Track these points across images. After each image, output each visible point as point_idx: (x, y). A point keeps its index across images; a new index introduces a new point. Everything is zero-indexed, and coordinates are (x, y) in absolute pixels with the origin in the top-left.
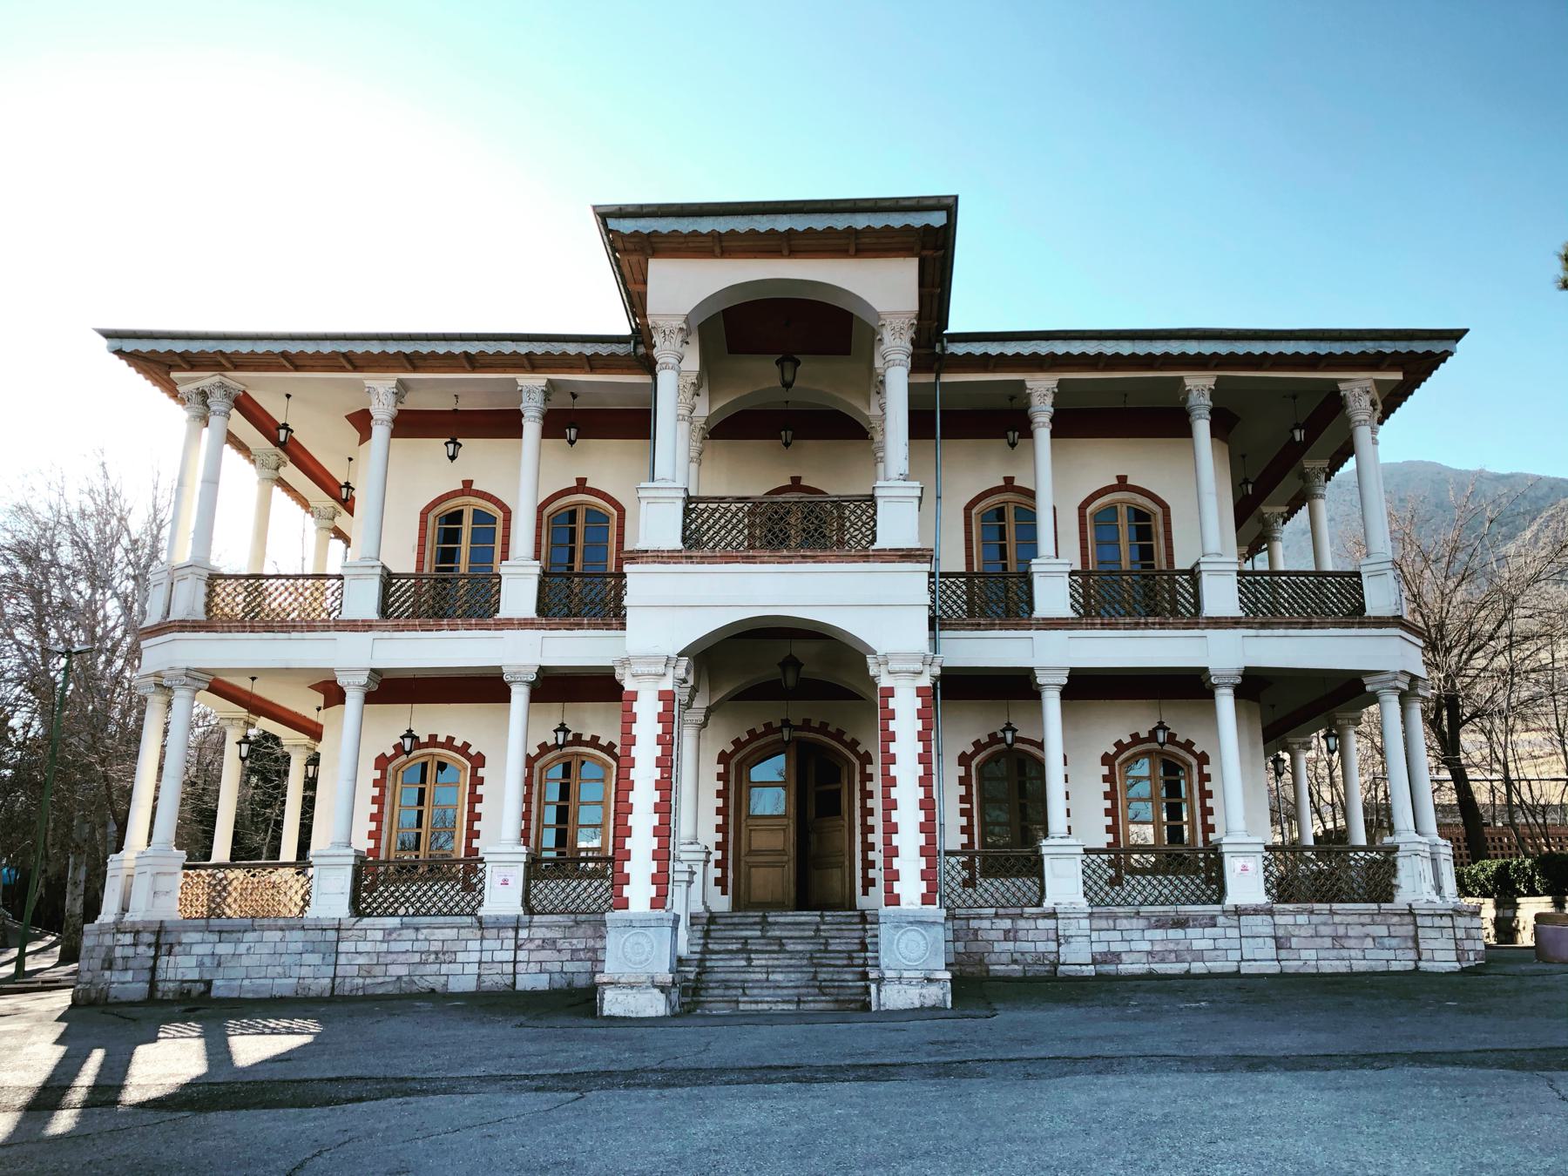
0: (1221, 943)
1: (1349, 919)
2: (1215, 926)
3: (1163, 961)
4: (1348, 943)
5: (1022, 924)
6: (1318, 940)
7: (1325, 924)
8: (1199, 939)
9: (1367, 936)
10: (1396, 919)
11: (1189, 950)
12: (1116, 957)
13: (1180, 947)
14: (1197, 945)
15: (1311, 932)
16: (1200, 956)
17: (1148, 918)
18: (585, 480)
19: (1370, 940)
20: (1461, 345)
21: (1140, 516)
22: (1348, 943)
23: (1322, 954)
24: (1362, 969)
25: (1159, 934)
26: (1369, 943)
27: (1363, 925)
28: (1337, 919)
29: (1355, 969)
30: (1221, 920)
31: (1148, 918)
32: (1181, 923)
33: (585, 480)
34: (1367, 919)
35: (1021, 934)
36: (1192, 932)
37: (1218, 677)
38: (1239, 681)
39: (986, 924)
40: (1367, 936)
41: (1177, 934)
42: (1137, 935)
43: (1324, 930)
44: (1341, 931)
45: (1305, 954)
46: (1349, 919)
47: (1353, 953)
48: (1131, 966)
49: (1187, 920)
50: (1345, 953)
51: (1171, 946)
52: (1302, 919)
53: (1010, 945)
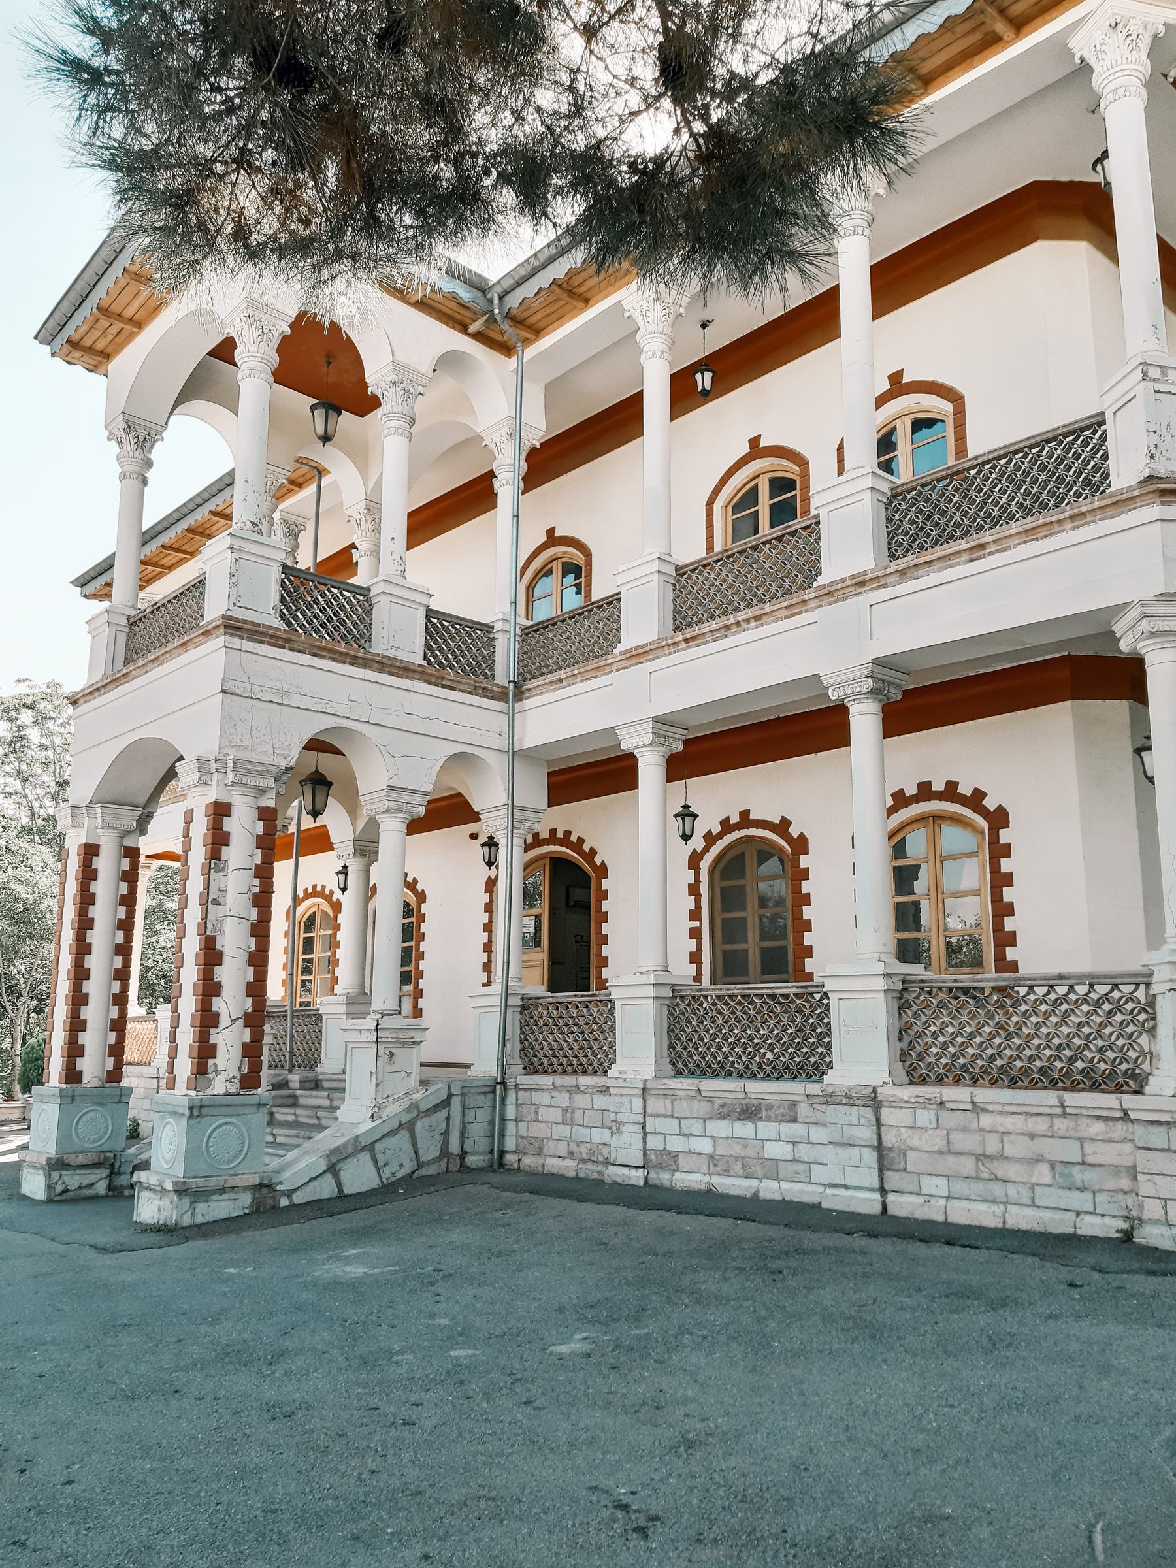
0: (803, 1152)
1: (1009, 1123)
2: (794, 1120)
3: (726, 1173)
4: (1002, 1169)
5: (580, 1100)
6: (951, 1159)
7: (965, 1129)
8: (772, 1139)
9: (1040, 1159)
10: (1098, 1128)
11: (761, 1158)
12: (670, 1159)
13: (750, 1152)
14: (776, 1150)
15: (940, 1143)
16: (772, 1169)
17: (711, 1100)
18: (902, 791)
19: (1044, 1168)
20: (1108, 427)
21: (780, 485)
22: (1002, 1169)
23: (960, 1187)
24: (1024, 1226)
25: (721, 1128)
26: (1043, 1174)
27: (1032, 1136)
28: (986, 1121)
29: (1012, 1223)
30: (803, 1110)
31: (711, 1100)
32: (749, 1113)
33: (902, 791)
34: (1041, 1125)
35: (578, 1115)
36: (767, 1129)
37: (840, 685)
38: (869, 684)
39: (545, 1098)
40: (1040, 1159)
41: (745, 1129)
42: (696, 1127)
43: (962, 1141)
44: (993, 1146)
45: (931, 1185)
46: (1009, 1123)
47: (1012, 1191)
48: (690, 1178)
49: (758, 1108)
50: (997, 1189)
51: (738, 1150)
52: (925, 1117)
53: (566, 1130)
